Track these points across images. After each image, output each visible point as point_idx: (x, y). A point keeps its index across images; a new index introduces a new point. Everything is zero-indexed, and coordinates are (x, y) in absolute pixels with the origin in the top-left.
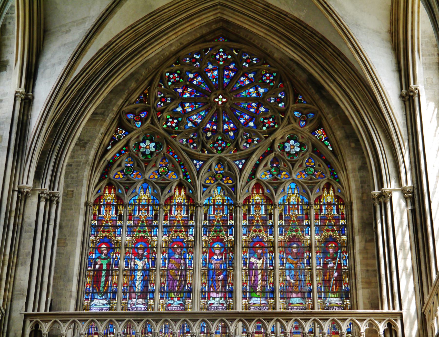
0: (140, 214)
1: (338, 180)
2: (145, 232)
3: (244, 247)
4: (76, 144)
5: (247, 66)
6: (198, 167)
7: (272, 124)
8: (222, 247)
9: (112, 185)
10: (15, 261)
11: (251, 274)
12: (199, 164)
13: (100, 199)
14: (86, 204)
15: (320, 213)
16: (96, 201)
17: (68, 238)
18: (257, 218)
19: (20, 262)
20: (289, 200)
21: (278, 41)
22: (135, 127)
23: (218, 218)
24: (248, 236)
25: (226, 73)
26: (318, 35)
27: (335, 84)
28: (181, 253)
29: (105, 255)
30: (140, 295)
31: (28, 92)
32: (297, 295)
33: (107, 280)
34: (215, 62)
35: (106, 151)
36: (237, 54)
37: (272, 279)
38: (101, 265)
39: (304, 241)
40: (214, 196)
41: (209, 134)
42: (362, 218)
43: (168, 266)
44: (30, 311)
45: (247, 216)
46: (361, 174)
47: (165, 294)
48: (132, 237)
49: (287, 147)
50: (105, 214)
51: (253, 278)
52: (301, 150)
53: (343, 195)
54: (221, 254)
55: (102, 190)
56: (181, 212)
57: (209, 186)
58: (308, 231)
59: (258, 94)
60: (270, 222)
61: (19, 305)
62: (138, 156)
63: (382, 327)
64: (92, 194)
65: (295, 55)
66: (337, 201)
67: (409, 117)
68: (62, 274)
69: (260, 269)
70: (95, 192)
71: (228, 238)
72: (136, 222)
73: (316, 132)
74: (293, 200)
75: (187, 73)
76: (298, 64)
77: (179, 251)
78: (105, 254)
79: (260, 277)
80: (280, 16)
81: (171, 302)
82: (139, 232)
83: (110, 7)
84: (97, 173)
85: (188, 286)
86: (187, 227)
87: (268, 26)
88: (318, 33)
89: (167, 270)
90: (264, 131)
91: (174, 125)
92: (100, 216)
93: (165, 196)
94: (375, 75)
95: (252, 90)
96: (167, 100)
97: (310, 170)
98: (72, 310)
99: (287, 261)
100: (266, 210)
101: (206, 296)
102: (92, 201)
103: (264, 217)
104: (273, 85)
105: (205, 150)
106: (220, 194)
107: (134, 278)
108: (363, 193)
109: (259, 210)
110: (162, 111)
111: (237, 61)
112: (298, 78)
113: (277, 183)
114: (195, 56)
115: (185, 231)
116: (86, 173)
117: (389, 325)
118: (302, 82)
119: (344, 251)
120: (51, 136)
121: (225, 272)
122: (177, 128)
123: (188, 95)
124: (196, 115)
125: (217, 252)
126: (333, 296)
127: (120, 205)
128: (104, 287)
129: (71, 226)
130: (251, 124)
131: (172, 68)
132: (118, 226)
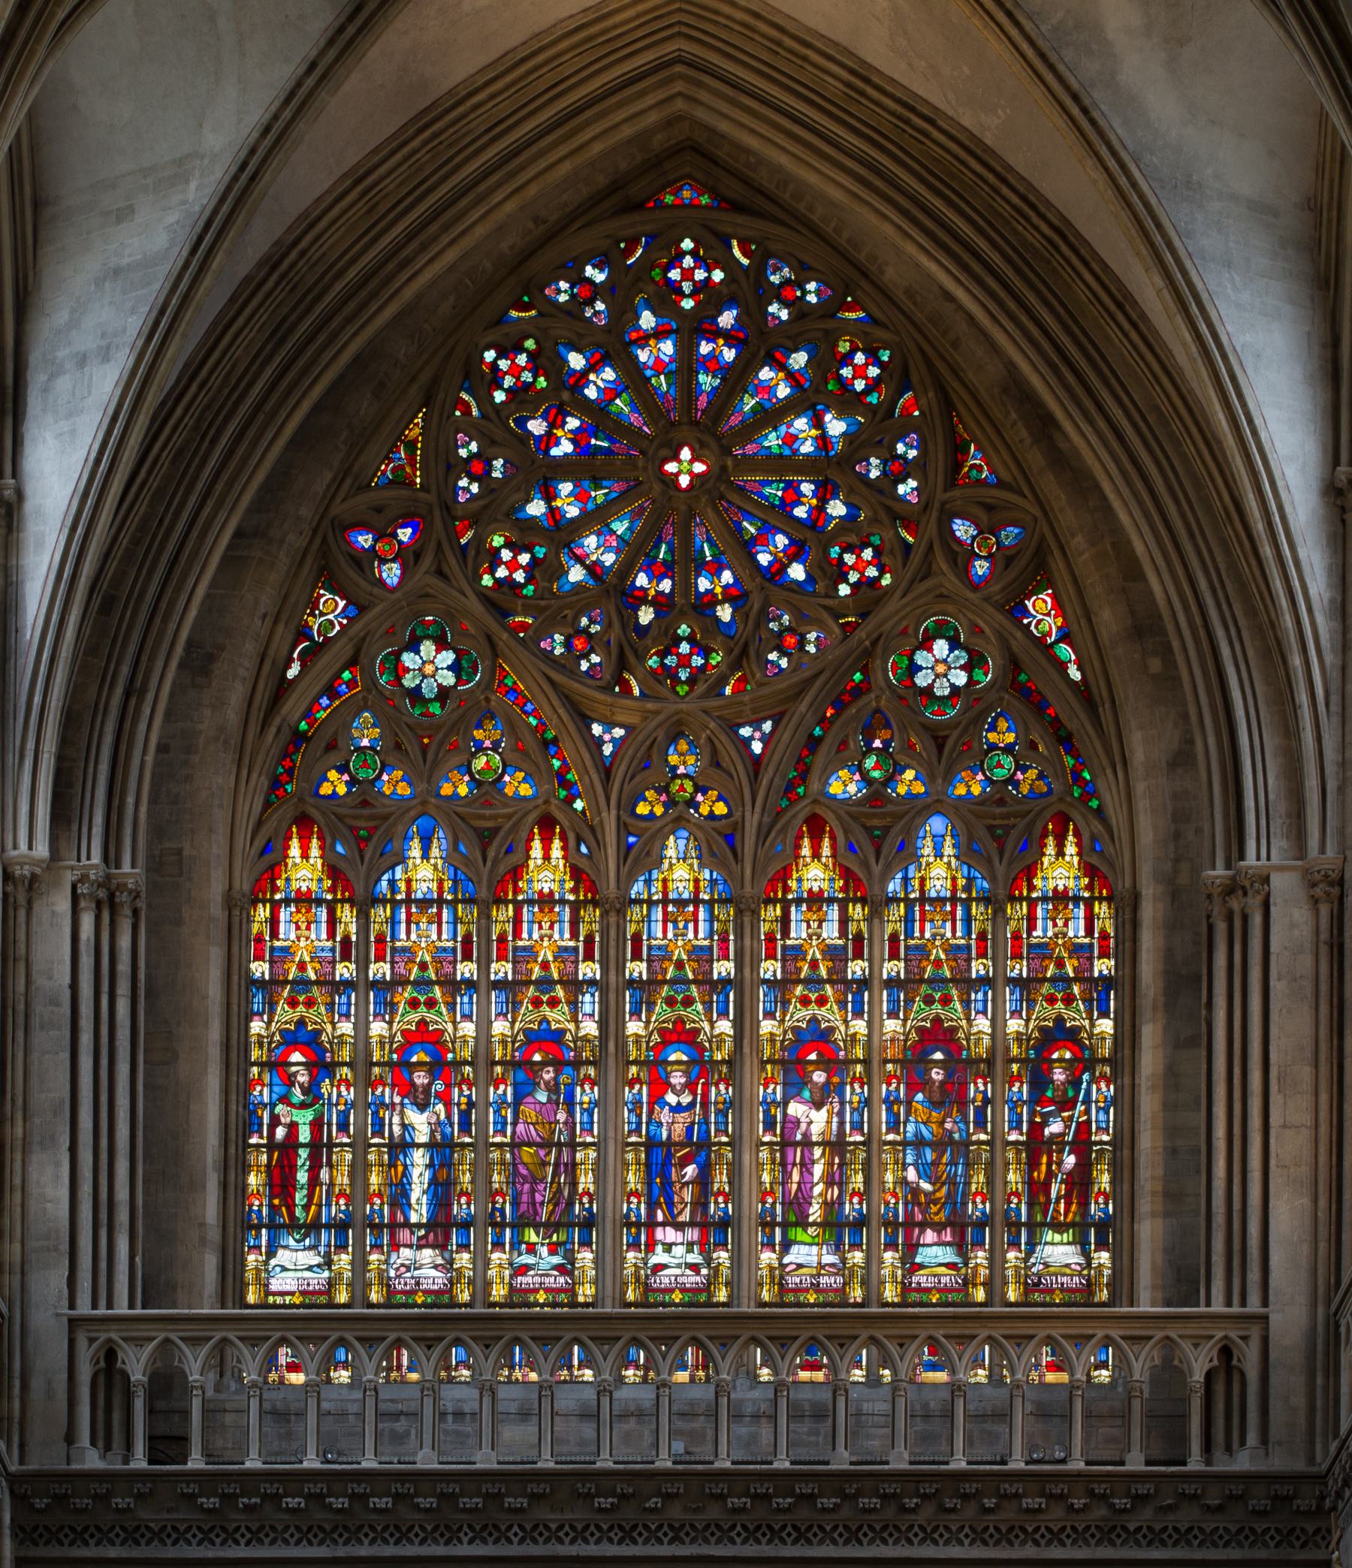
0: (413, 937)
2: (431, 1004)
3: (768, 1061)
4: (181, 666)
7: (872, 572)
8: (690, 1063)
9: (313, 822)
11: (790, 1160)
15: (1029, 935)
18: (814, 952)
20: (923, 880)
23: (679, 953)
24: (782, 1021)
25: (705, 348)
26: (1049, 215)
28: (557, 1084)
32: (939, 1233)
34: (665, 297)
42: (1169, 955)
43: (514, 1132)
44: (84, 1308)
47: (508, 1231)
49: (921, 668)
50: (293, 937)
51: (796, 1177)
52: (971, 682)
53: (1111, 865)
54: (691, 1086)
56: (551, 927)
58: (985, 1001)
59: (823, 441)
66: (1089, 887)
69: (818, 1144)
71: (712, 1028)
72: (401, 969)
73: (1029, 604)
74: (938, 884)
75: (562, 349)
76: (971, 318)
79: (818, 1170)
80: (907, 122)
81: (527, 1259)
82: (414, 1004)
85: (581, 1203)
86: (575, 986)
87: (861, 162)
88: (1049, 204)
91: (519, 576)
95: (801, 424)
96: (490, 468)
97: (1000, 765)
99: (908, 1113)
100: (844, 921)
101: (643, 1238)
102: (246, 887)
103: (835, 947)
106: (684, 859)
108: (1177, 860)
109: (821, 922)
112: (970, 375)
113: (883, 816)
114: (589, 271)
119: (1103, 1076)
122: (531, 588)
124: (599, 534)
125: (677, 1079)
127: (343, 901)
131: (506, 329)
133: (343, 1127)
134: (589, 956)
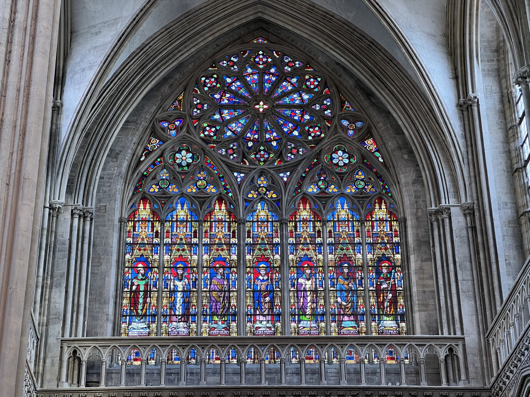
0: (178, 231)
1: (390, 195)
2: (183, 250)
4: (108, 156)
5: (289, 69)
6: (239, 180)
7: (318, 133)
10: (49, 282)
11: (300, 296)
12: (240, 177)
13: (134, 215)
14: (121, 221)
16: (130, 216)
17: (102, 257)
19: (54, 284)
21: (324, 44)
22: (169, 137)
23: (262, 235)
25: (266, 77)
27: (387, 91)
28: (224, 273)
29: (143, 275)
30: (181, 319)
31: (56, 99)
32: (349, 317)
33: (145, 302)
35: (139, 163)
36: (278, 57)
37: (323, 301)
38: (138, 286)
39: (355, 261)
40: (258, 210)
41: (250, 144)
43: (210, 288)
45: (294, 233)
46: (416, 188)
47: (208, 317)
48: (171, 256)
49: (334, 158)
51: (302, 301)
53: (397, 211)
54: (267, 274)
55: (137, 205)
57: (252, 201)
59: (302, 100)
60: (319, 240)
61: (55, 329)
62: (175, 168)
63: (442, 353)
64: (126, 209)
65: (343, 60)
67: (467, 128)
68: (96, 295)
70: (129, 207)
72: (174, 240)
76: (345, 69)
77: (221, 270)
78: (141, 274)
79: (309, 299)
81: (215, 326)
82: (178, 250)
83: (144, 7)
84: (130, 186)
86: (229, 245)
89: (209, 291)
90: (310, 141)
92: (135, 233)
93: (205, 211)
94: (431, 83)
97: (360, 184)
98: (109, 336)
99: (337, 282)
100: (314, 227)
102: (126, 217)
104: (318, 91)
105: (247, 162)
107: (174, 300)
110: (199, 119)
111: (279, 64)
113: (325, 197)
114: (232, 59)
115: (227, 250)
116: (119, 186)
117: (451, 350)
118: (349, 88)
119: (399, 271)
120: (82, 147)
121: (272, 294)
123: (226, 101)
125: (263, 272)
126: (388, 319)
127: (156, 221)
128: (142, 310)
129: (105, 244)
130: (296, 133)
132: (155, 244)
133: (155, 286)
134: (234, 237)
